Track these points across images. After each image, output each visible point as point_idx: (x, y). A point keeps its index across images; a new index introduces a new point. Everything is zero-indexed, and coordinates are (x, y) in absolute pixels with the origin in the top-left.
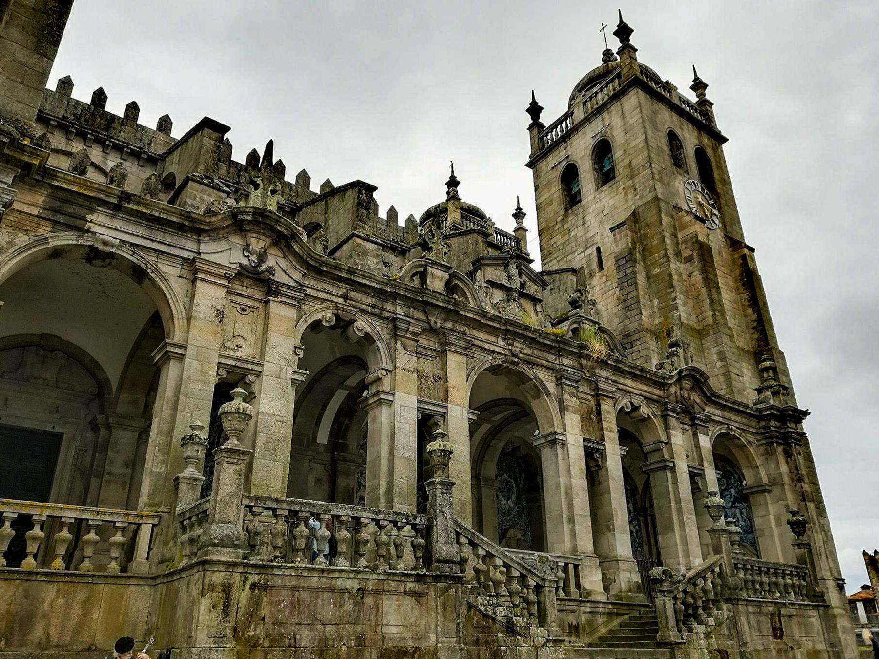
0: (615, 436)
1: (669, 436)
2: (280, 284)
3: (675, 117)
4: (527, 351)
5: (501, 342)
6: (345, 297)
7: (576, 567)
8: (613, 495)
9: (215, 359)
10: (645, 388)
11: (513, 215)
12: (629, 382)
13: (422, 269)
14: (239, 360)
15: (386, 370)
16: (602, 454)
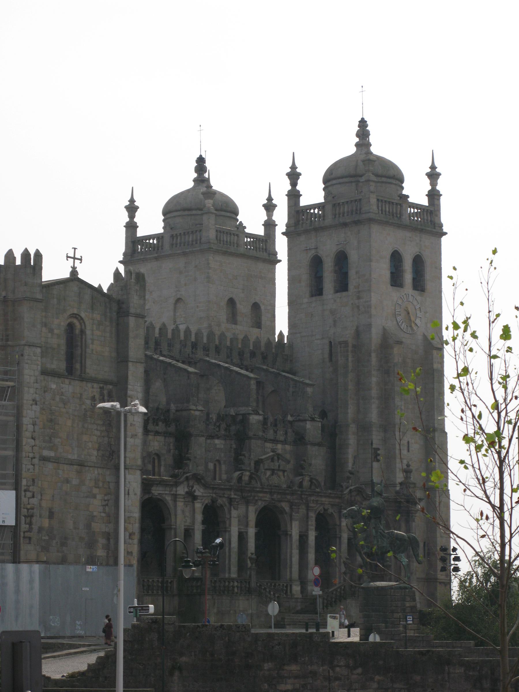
0: (313, 527)
1: (340, 522)
2: (198, 496)
3: (401, 234)
4: (279, 497)
5: (268, 496)
6: (215, 493)
7: (291, 586)
8: (309, 554)
9: (183, 528)
10: (331, 500)
11: (264, 206)
12: (324, 499)
13: (241, 475)
14: (188, 526)
15: (227, 518)
16: (307, 536)
